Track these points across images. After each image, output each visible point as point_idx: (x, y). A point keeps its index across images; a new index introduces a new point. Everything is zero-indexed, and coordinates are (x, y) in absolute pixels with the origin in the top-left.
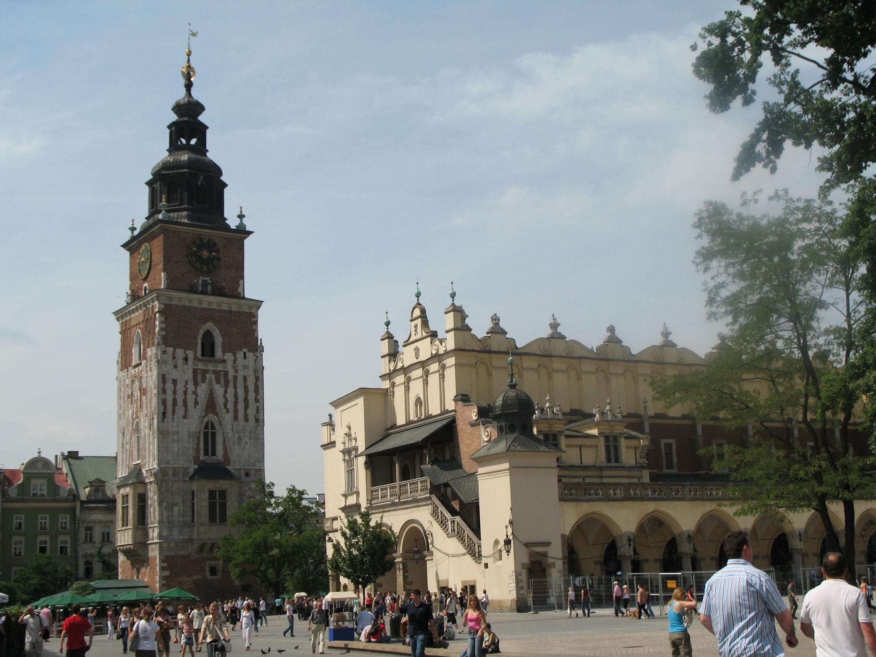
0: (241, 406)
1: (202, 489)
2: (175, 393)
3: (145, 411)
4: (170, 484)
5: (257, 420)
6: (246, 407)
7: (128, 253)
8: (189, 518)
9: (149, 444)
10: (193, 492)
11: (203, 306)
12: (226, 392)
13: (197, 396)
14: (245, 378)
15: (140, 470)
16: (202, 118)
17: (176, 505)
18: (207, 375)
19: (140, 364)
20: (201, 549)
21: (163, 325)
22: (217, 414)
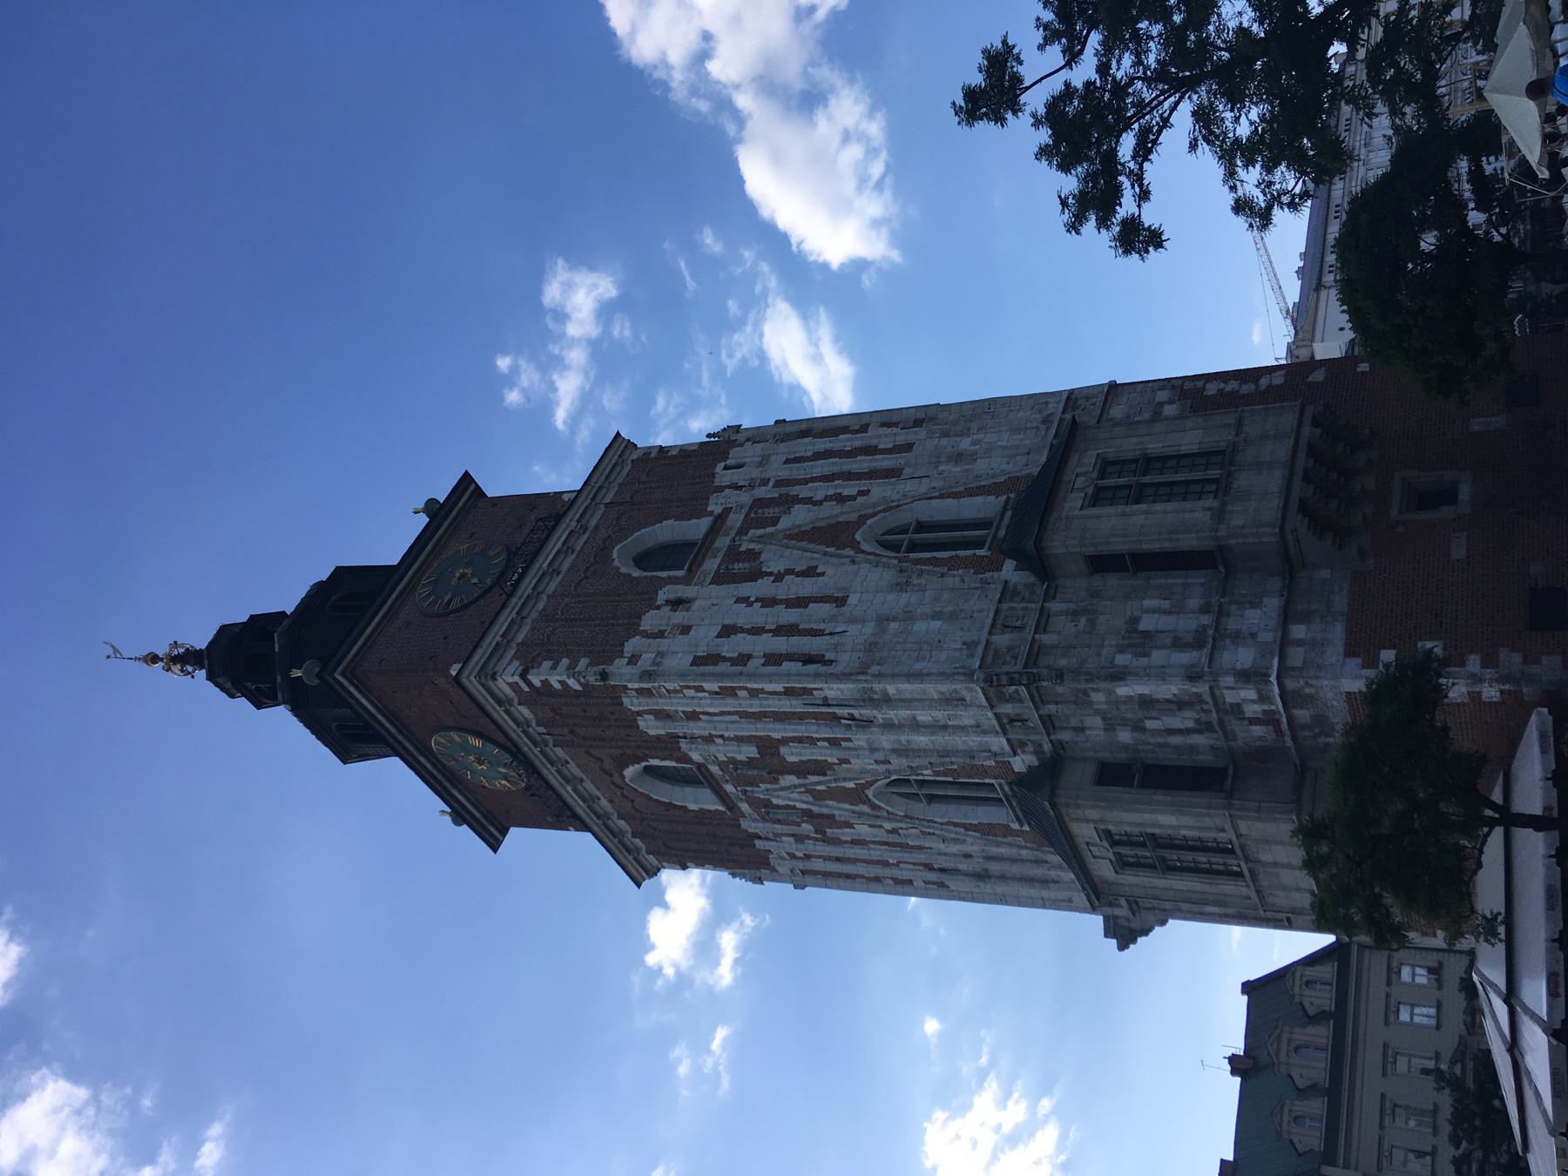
0: (862, 464)
1: (1084, 526)
2: (757, 631)
3: (822, 753)
4: (1047, 639)
5: (918, 423)
6: (871, 450)
7: (514, 832)
8: (1197, 579)
9: (915, 726)
11: (565, 566)
12: (809, 501)
13: (790, 572)
14: (788, 461)
15: (1023, 782)
17: (1135, 620)
18: (743, 548)
21: (565, 662)
22: (862, 519)
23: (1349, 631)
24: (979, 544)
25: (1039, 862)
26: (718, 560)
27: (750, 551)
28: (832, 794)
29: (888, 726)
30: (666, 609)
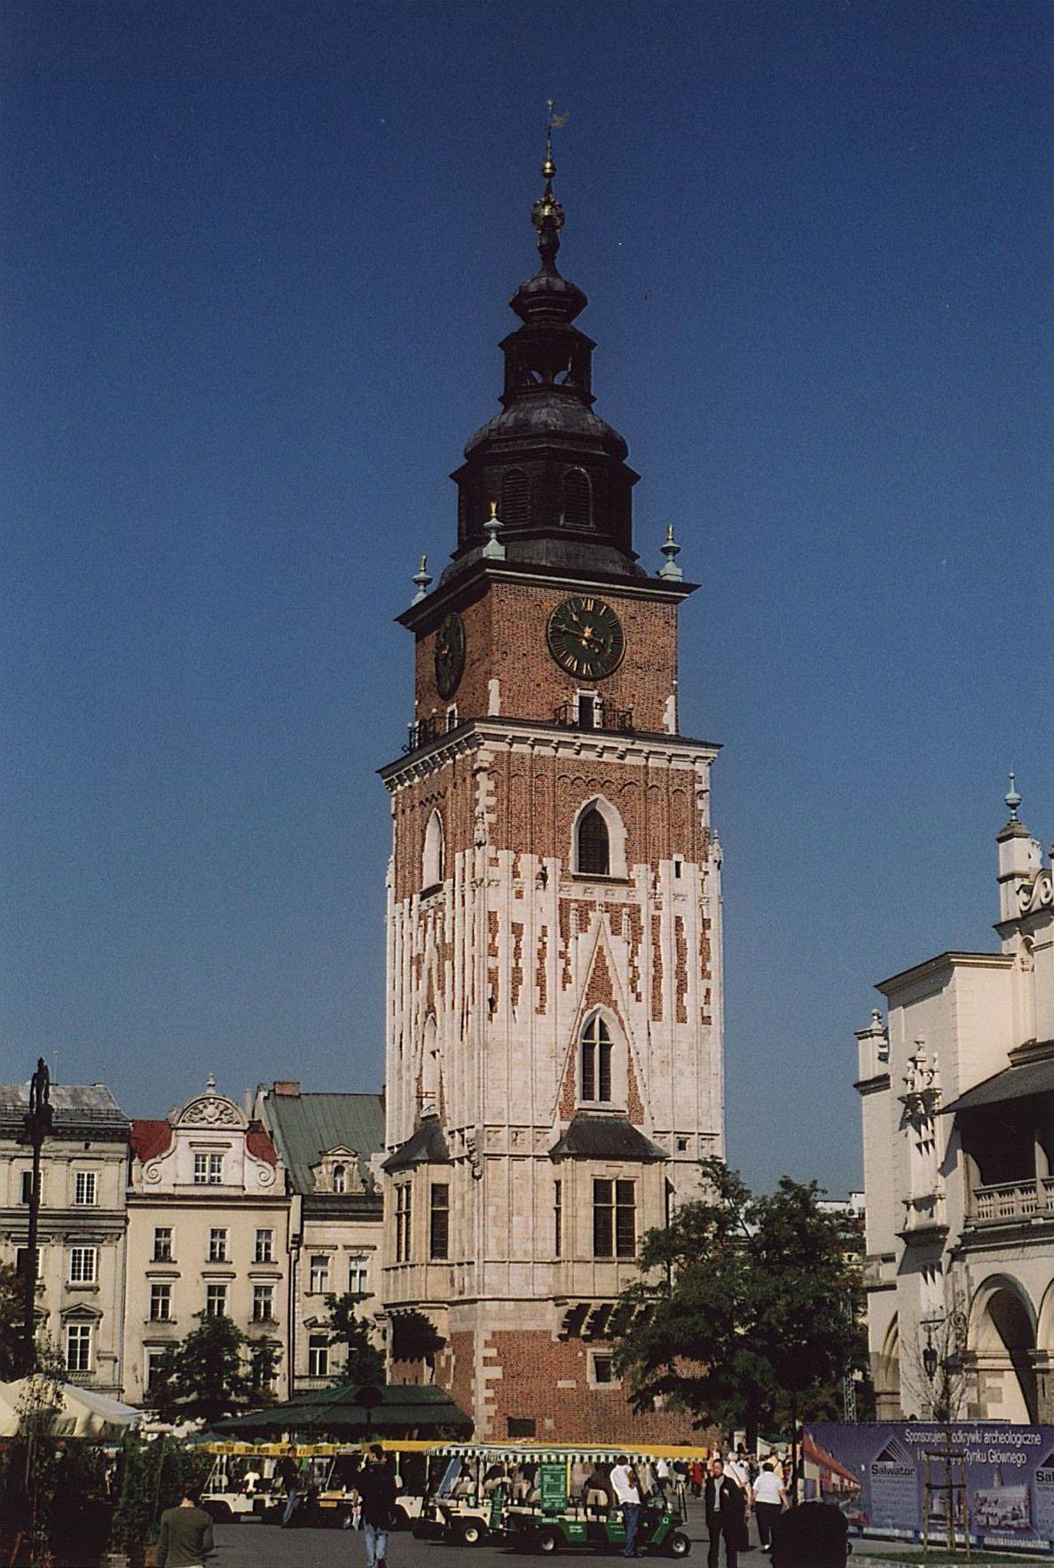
0: (668, 985)
2: (517, 953)
5: (706, 1020)
6: (681, 989)
10: (558, 1183)
13: (568, 964)
14: (678, 919)
16: (578, 324)
18: (591, 914)
19: (437, 889)
20: (573, 1320)
21: (492, 801)
23: (508, 1333)
24: (587, 1095)
25: (408, 1118)
26: (580, 898)
27: (588, 922)
28: (430, 987)
29: (461, 1052)
30: (539, 868)
